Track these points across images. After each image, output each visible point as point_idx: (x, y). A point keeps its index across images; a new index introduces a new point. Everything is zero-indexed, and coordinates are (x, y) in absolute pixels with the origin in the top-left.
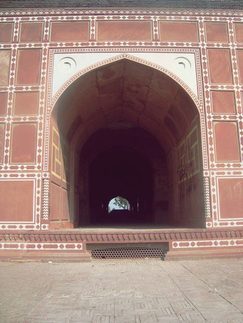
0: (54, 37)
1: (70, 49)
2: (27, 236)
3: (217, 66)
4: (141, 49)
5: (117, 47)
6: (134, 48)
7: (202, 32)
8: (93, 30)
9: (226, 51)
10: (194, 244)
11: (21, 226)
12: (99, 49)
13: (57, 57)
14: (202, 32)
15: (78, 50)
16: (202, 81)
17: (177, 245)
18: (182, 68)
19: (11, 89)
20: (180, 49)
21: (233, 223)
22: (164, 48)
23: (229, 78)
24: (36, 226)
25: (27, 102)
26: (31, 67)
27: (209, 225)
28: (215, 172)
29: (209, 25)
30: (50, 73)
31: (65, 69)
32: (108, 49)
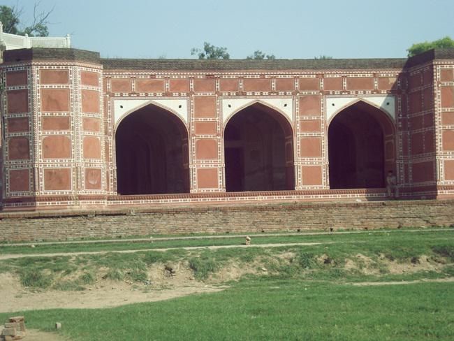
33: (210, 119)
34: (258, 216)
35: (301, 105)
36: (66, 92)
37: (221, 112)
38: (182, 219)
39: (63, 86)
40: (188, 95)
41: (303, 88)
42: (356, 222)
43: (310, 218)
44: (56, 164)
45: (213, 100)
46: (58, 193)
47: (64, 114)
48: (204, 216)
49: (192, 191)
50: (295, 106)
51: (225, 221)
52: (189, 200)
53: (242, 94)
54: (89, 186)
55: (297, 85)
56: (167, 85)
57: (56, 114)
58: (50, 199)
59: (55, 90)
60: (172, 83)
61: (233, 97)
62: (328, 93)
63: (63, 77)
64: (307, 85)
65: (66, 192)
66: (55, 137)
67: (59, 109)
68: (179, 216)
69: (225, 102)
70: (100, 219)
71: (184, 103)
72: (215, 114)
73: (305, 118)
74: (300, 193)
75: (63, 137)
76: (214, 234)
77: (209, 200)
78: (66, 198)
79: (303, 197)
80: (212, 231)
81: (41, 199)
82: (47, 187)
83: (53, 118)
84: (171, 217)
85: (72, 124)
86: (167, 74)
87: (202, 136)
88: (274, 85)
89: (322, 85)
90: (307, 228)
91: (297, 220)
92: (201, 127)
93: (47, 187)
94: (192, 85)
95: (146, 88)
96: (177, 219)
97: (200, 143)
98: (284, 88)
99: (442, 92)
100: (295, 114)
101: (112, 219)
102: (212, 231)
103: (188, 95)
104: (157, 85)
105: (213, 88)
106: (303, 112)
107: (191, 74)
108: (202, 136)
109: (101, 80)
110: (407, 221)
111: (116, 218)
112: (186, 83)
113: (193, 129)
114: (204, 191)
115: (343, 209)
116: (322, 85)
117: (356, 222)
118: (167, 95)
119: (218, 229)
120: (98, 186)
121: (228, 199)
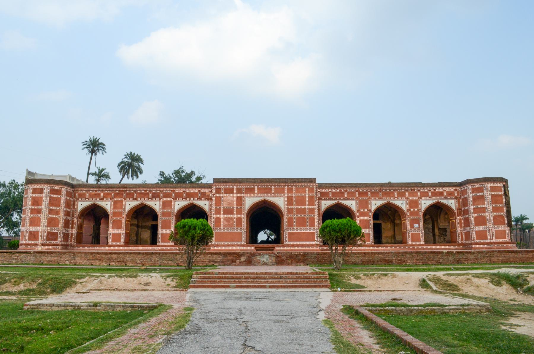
0: (246, 193)
1: (250, 196)
2: (241, 245)
3: (289, 201)
4: (269, 196)
5: (262, 196)
6: (267, 196)
7: (286, 191)
8: (256, 191)
9: (292, 197)
10: (281, 248)
11: (239, 243)
12: (258, 196)
13: (247, 198)
14: (286, 191)
15: (252, 196)
16: (285, 205)
17: (277, 248)
18: (280, 201)
19: (235, 207)
20: (280, 196)
21: (291, 243)
22: (275, 196)
23: (292, 205)
24: (243, 243)
25: (239, 212)
26: (240, 201)
27: (284, 243)
28: (286, 230)
29: (288, 189)
30: (245, 203)
31: (250, 201)
32: (260, 197)
33: (120, 211)
34: (90, 257)
36: (42, 197)
37: (125, 207)
38: (54, 257)
39: (40, 195)
40: (111, 199)
41: (164, 197)
42: (138, 262)
43: (116, 259)
44: (34, 229)
45: (122, 201)
46: (33, 242)
47: (40, 207)
48: (64, 256)
50: (160, 205)
52: (107, 248)
53: (135, 199)
54: (48, 239)
55: (161, 195)
56: (102, 195)
57: (36, 207)
59: (37, 197)
60: (104, 194)
61: (131, 201)
62: (176, 199)
63: (41, 191)
64: (166, 195)
65: (36, 242)
66: (35, 217)
67: (38, 205)
68: (53, 255)
69: (128, 203)
70: (18, 255)
71: (109, 203)
72: (122, 208)
73: (165, 211)
74: (159, 246)
75: (38, 217)
76: (69, 265)
77: (116, 248)
78: (36, 245)
79: (160, 248)
80: (68, 263)
81: (21, 245)
82: (29, 239)
83: (35, 209)
84: (49, 255)
86: (102, 190)
87: (115, 218)
88: (150, 195)
89: (173, 195)
90: (114, 264)
91: (109, 259)
93: (29, 239)
94: (113, 195)
95: (92, 196)
96: (52, 257)
99: (216, 199)
100: (160, 209)
101: (23, 255)
102: (68, 263)
103: (111, 199)
104: (98, 195)
105: (122, 197)
106: (163, 208)
107: (113, 190)
108: (115, 218)
109: (64, 193)
110: (165, 262)
111: (24, 255)
112: (110, 194)
113: (112, 215)
114: (114, 243)
115: (132, 255)
116: (173, 195)
117: (138, 262)
118: (102, 199)
119: (70, 262)
120: (56, 239)
121: (124, 248)
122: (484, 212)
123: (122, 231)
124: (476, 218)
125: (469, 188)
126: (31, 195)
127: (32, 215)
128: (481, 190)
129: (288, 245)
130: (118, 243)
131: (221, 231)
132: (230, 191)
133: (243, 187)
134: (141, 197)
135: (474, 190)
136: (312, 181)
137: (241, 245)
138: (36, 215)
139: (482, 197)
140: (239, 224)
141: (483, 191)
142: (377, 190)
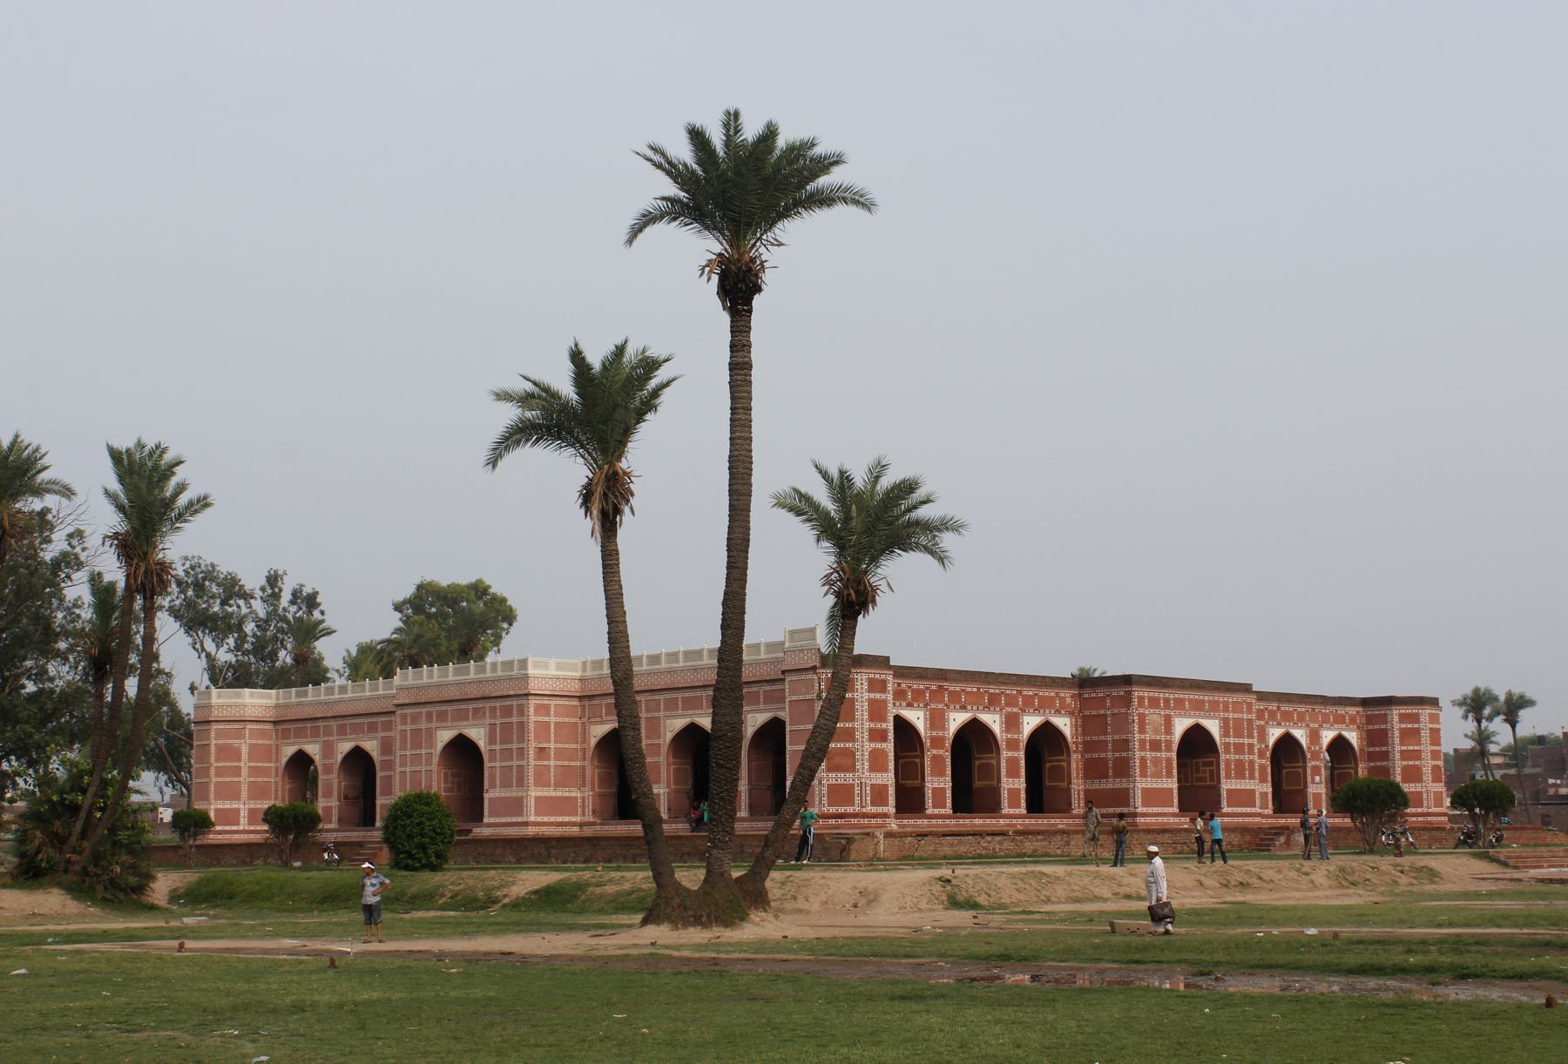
1: (1180, 716)
12: (1189, 716)
18: (1213, 726)
22: (1209, 717)
25: (1169, 743)
26: (1168, 722)
35: (1083, 726)
49: (929, 811)
51: (1068, 844)
52: (925, 821)
58: (875, 816)
60: (913, 691)
65: (885, 809)
71: (921, 714)
77: (940, 821)
78: (885, 816)
85: (858, 735)
92: (937, 742)
97: (935, 757)
98: (993, 703)
105: (942, 701)
108: (935, 752)
109: (890, 687)
114: (936, 811)
118: (910, 705)
121: (953, 822)
122: (1419, 758)
123: (946, 783)
124: (1405, 769)
125: (1395, 713)
126: (866, 695)
127: (873, 745)
128: (1415, 718)
129: (1228, 815)
130: (942, 811)
131: (1110, 786)
132: (1154, 703)
133: (1172, 695)
134: (972, 704)
135: (1403, 718)
136: (1246, 688)
137: (1174, 815)
138: (879, 745)
139: (1417, 732)
140: (1169, 775)
141: (1418, 721)
142: (1273, 706)
